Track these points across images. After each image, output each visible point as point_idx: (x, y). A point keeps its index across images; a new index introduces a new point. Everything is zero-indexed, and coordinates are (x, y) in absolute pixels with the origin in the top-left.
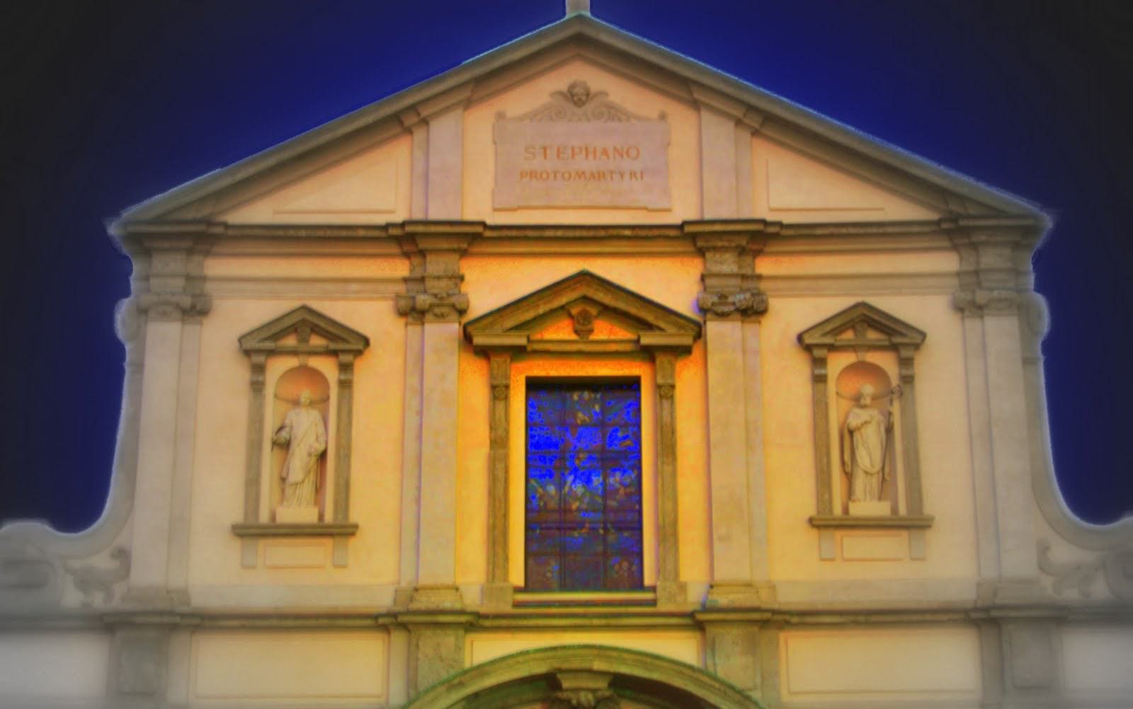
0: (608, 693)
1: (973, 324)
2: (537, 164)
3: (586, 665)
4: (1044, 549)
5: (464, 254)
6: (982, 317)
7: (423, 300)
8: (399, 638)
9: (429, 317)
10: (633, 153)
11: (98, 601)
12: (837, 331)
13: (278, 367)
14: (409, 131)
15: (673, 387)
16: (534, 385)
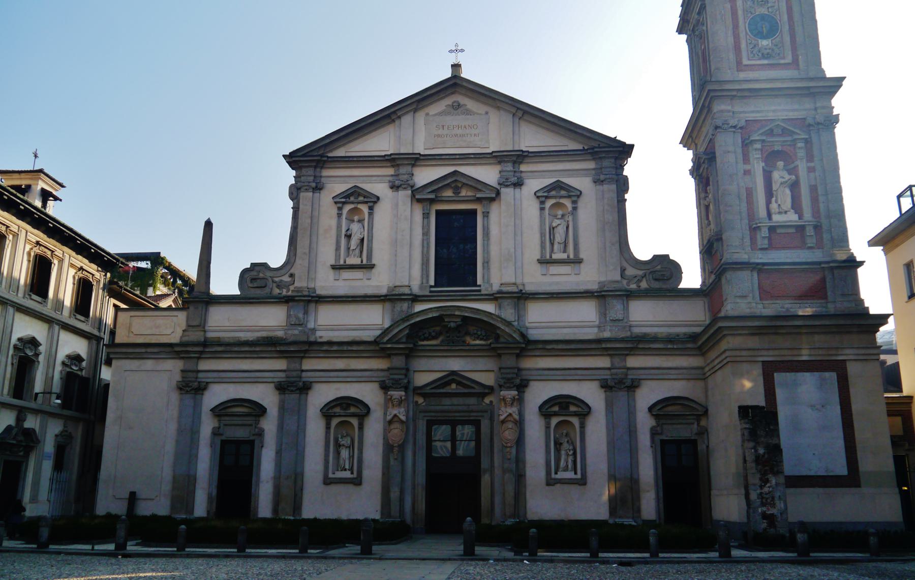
0: (460, 323)
1: (600, 187)
2: (440, 132)
3: (453, 313)
4: (623, 270)
5: (413, 165)
6: (603, 185)
7: (397, 183)
8: (388, 305)
9: (400, 189)
10: (475, 127)
11: (284, 292)
12: (549, 191)
13: (347, 208)
14: (393, 121)
15: (488, 212)
16: (439, 213)
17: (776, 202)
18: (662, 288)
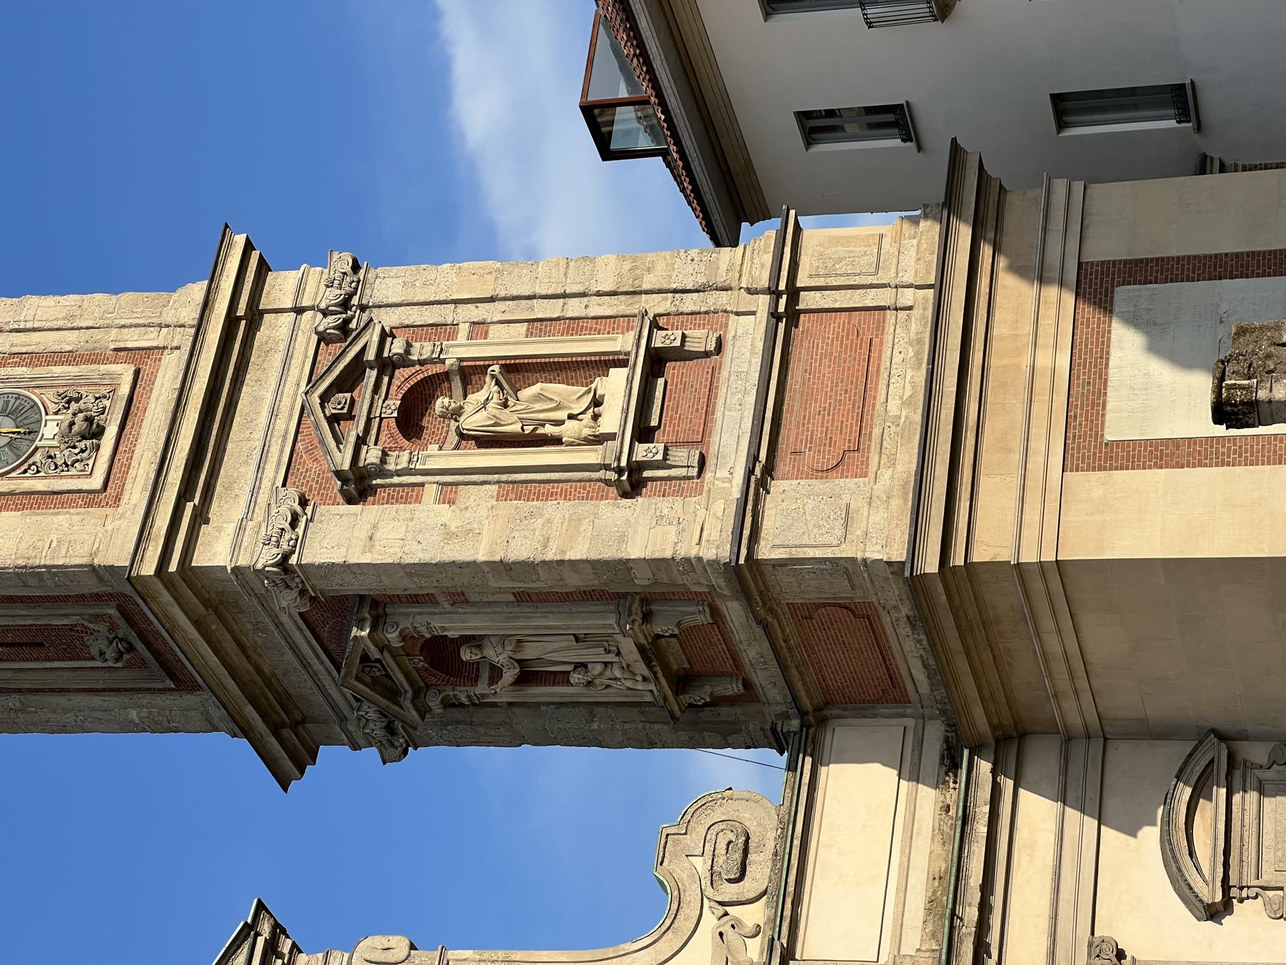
17: (559, 423)
18: (776, 854)
